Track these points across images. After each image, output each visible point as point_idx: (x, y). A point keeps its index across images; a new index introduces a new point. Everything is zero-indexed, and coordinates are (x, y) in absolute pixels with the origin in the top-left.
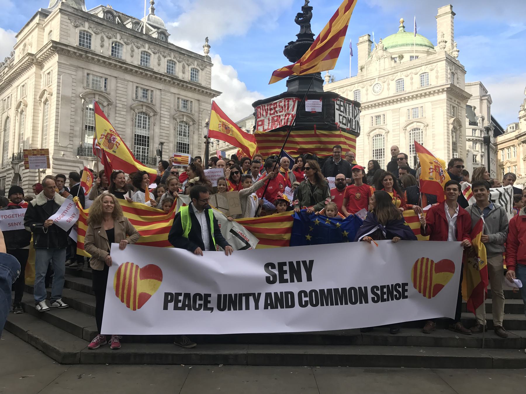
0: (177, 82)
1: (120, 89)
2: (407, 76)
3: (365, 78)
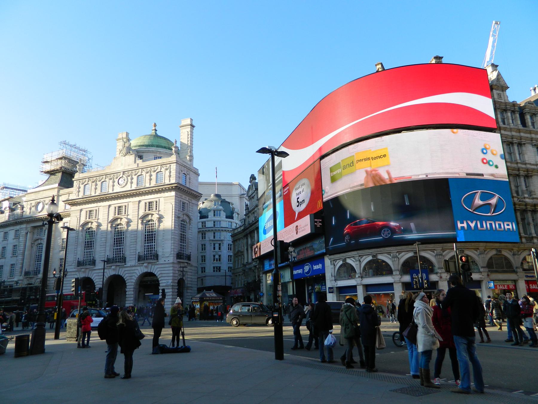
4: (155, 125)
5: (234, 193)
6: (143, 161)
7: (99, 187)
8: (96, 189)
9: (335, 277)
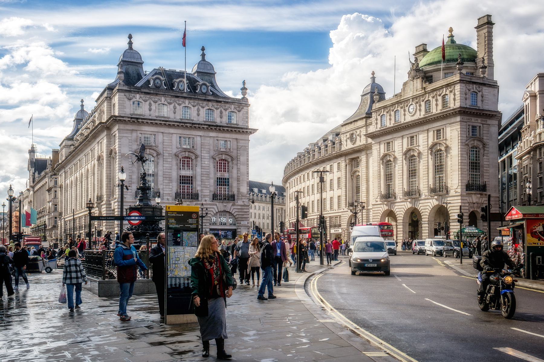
0: (213, 128)
1: (165, 141)
2: (433, 97)
3: (402, 98)
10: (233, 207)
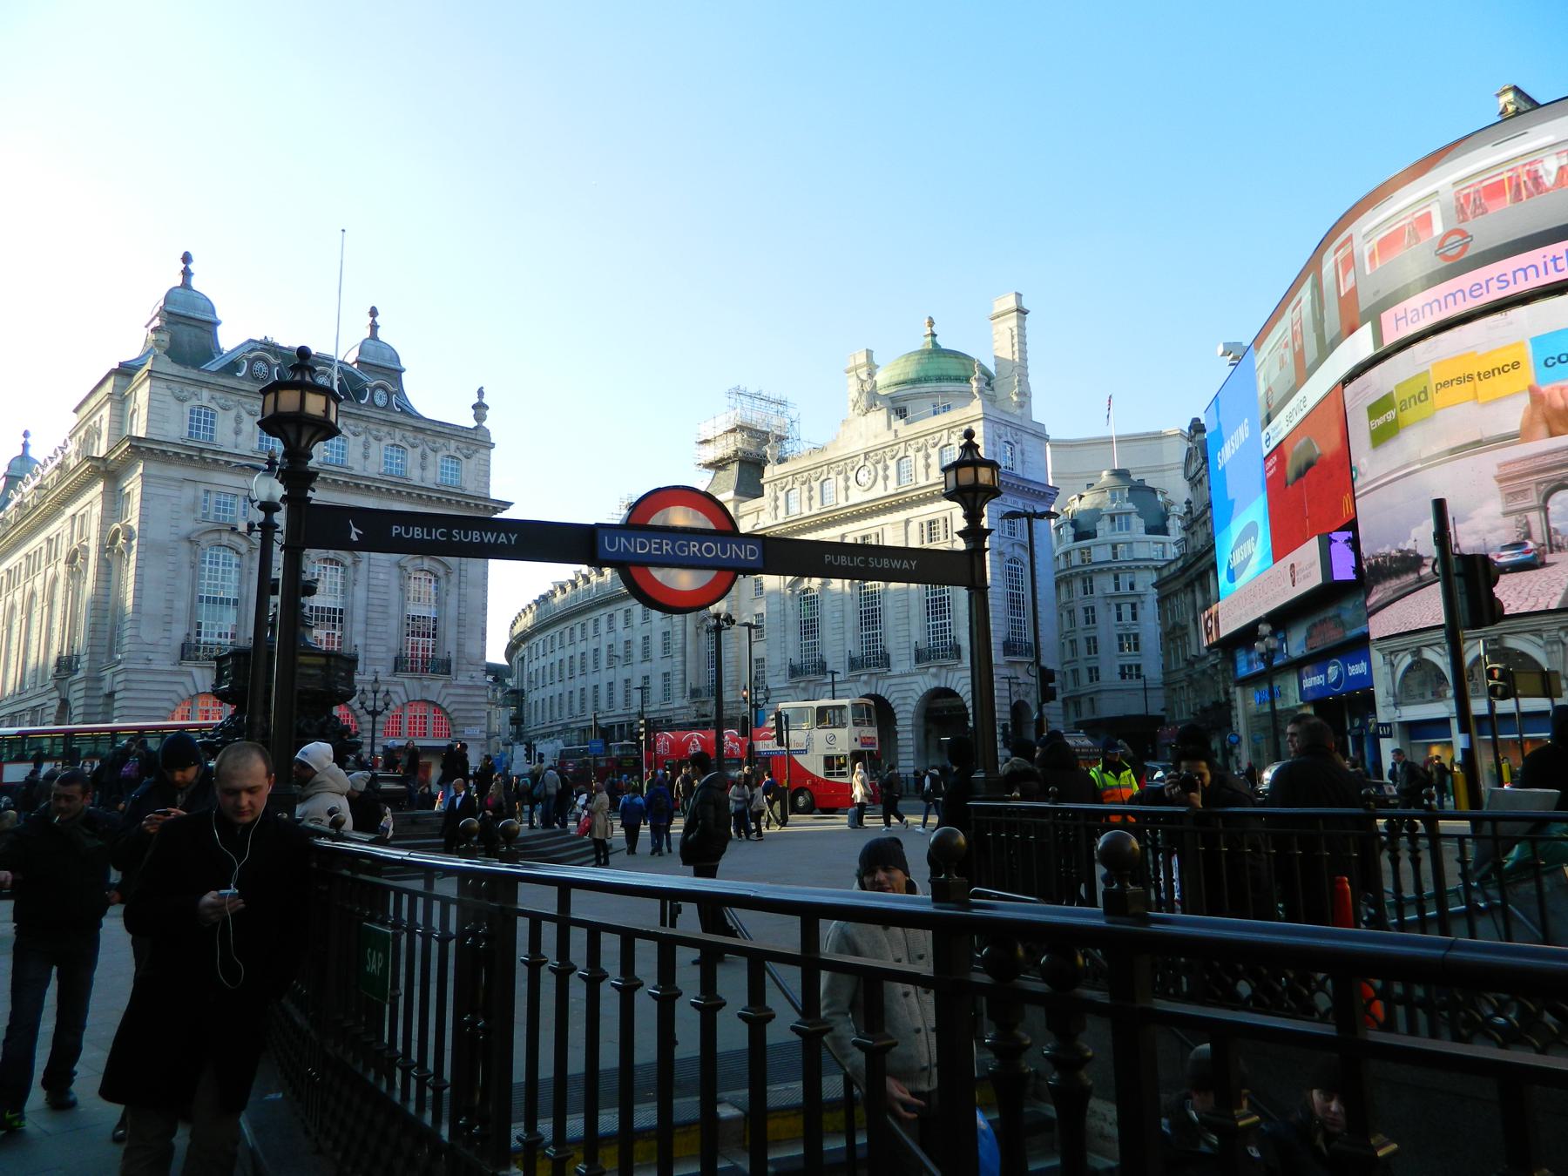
4: (931, 323)
5: (1167, 461)
6: (908, 423)
7: (816, 493)
8: (810, 498)
9: (1394, 695)
10: (444, 692)
